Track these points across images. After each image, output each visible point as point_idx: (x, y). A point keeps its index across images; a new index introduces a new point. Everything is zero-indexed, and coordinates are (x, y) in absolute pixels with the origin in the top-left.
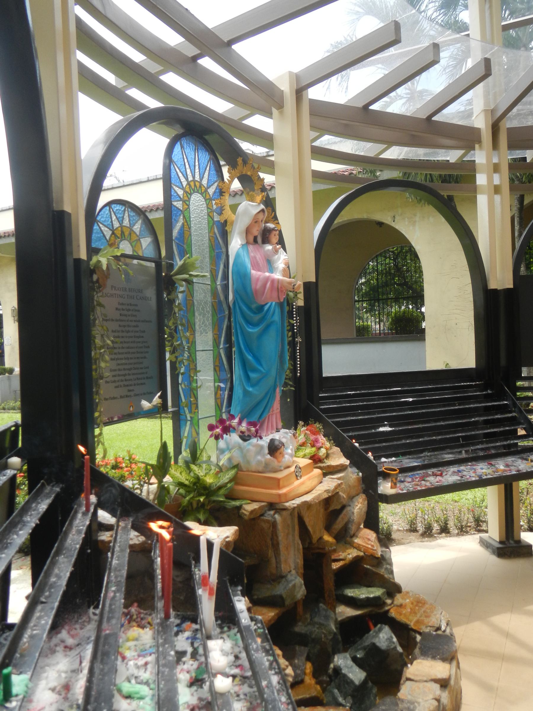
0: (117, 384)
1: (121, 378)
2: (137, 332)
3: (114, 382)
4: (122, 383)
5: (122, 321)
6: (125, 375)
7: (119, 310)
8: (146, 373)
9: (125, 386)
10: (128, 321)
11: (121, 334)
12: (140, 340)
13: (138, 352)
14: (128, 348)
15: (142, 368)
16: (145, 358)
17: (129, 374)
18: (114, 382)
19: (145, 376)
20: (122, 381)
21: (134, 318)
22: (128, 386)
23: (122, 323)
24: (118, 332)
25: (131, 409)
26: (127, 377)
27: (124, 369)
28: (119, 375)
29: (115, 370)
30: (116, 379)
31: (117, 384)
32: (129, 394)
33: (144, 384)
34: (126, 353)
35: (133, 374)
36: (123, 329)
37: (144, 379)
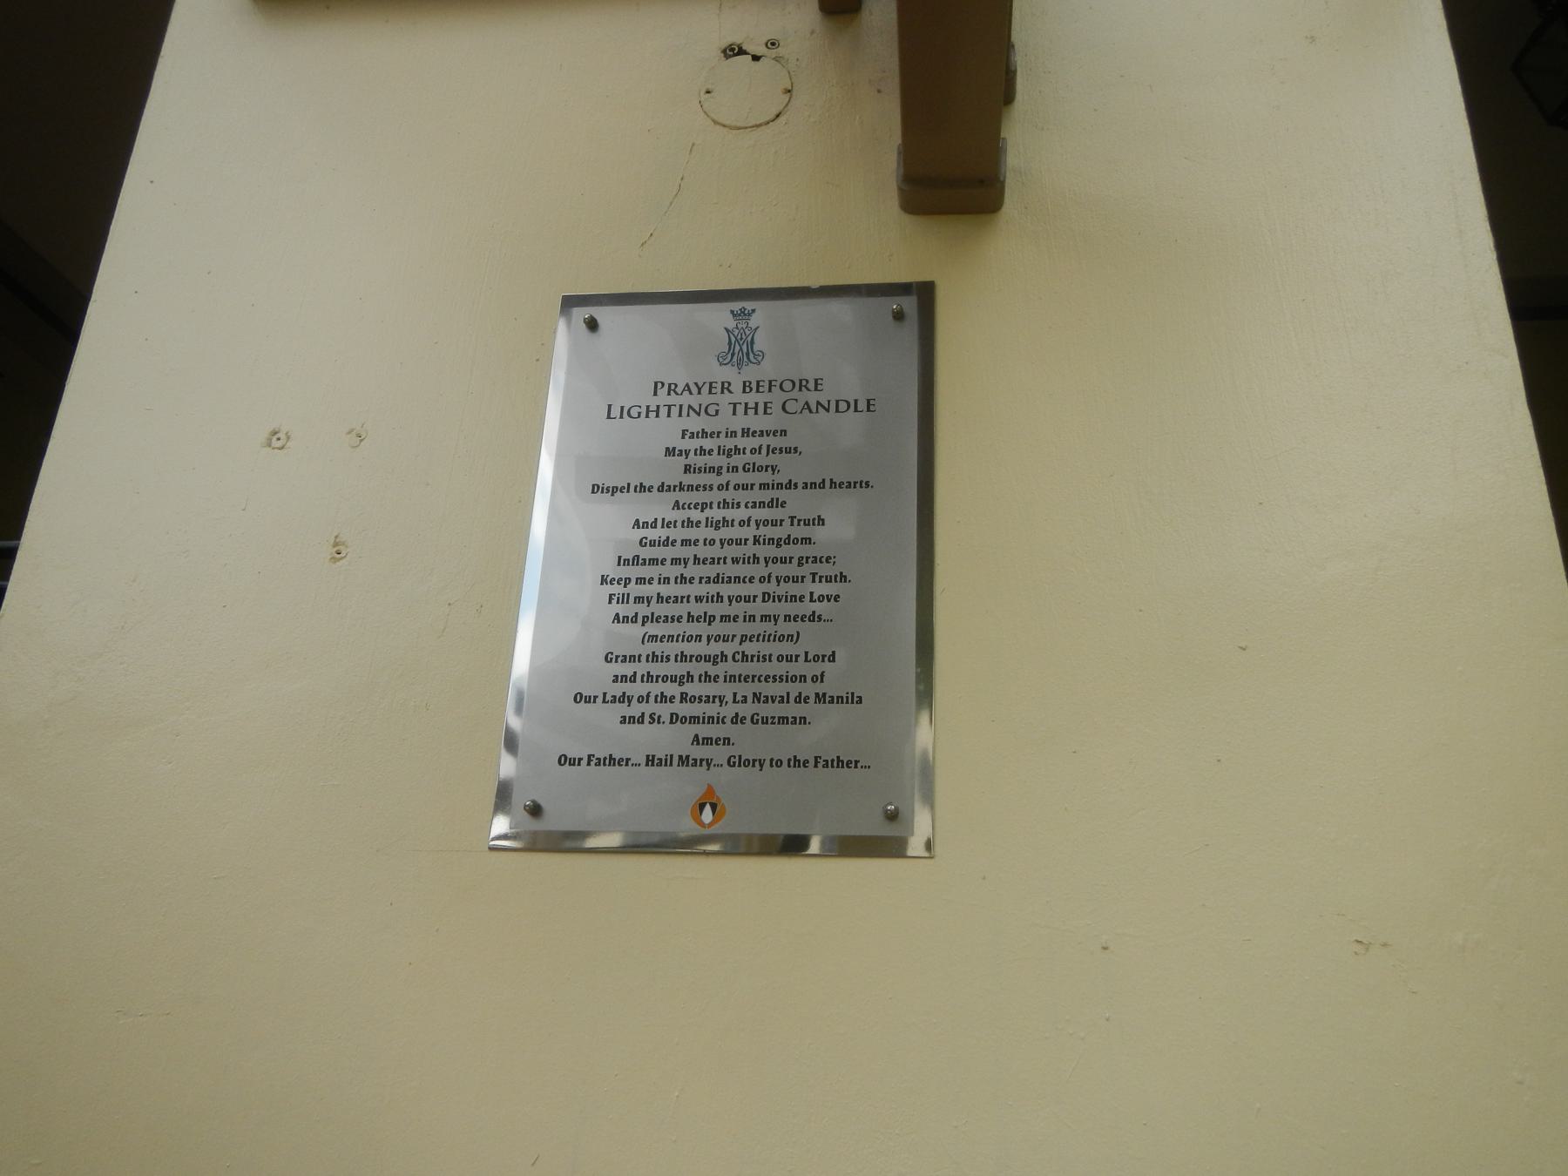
3: (624, 699)
4: (664, 710)
5: (690, 488)
6: (679, 680)
9: (674, 718)
11: (678, 534)
12: (796, 551)
13: (766, 597)
16: (813, 617)
18: (624, 699)
19: (809, 689)
20: (663, 698)
21: (766, 477)
23: (684, 497)
27: (683, 657)
29: (633, 659)
31: (636, 709)
33: (803, 720)
35: (732, 679)
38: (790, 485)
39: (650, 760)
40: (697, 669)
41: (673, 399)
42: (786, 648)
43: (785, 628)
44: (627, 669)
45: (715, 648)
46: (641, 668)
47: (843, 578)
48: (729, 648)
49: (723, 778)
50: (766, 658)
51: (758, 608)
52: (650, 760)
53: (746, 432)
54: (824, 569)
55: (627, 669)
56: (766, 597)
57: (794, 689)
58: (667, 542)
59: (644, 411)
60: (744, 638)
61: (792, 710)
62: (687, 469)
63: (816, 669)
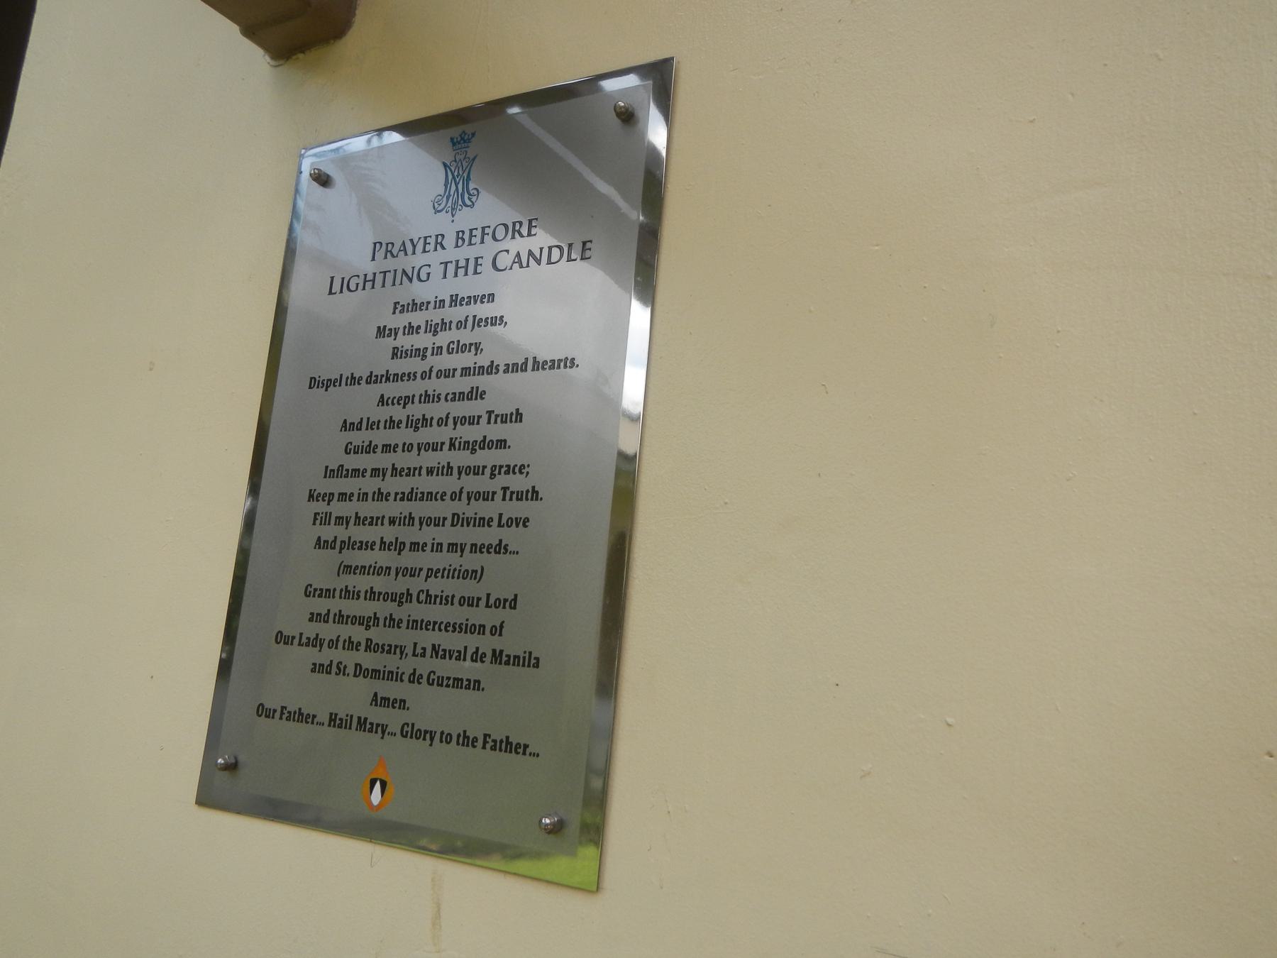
0: (326, 655)
1: (346, 631)
2: (473, 421)
3: (316, 642)
4: (350, 659)
6: (368, 622)
7: (394, 332)
8: (498, 630)
9: (359, 671)
13: (457, 520)
14: (410, 496)
15: (471, 602)
16: (501, 548)
17: (392, 622)
18: (316, 642)
19: (487, 643)
20: (351, 645)
22: (375, 674)
23: (392, 390)
24: (372, 425)
25: (376, 796)
26: (379, 635)
27: (372, 595)
28: (341, 618)
29: (327, 593)
30: (328, 631)
31: (326, 655)
32: (377, 715)
34: (392, 522)
36: (398, 413)
37: (478, 657)
39: (333, 719)
41: (390, 264)
45: (400, 585)
46: (335, 605)
47: (535, 494)
48: (416, 584)
50: (448, 600)
51: (446, 535)
52: (334, 720)
56: (457, 520)
59: (361, 281)
60: (432, 573)
61: (467, 669)
62: (395, 353)
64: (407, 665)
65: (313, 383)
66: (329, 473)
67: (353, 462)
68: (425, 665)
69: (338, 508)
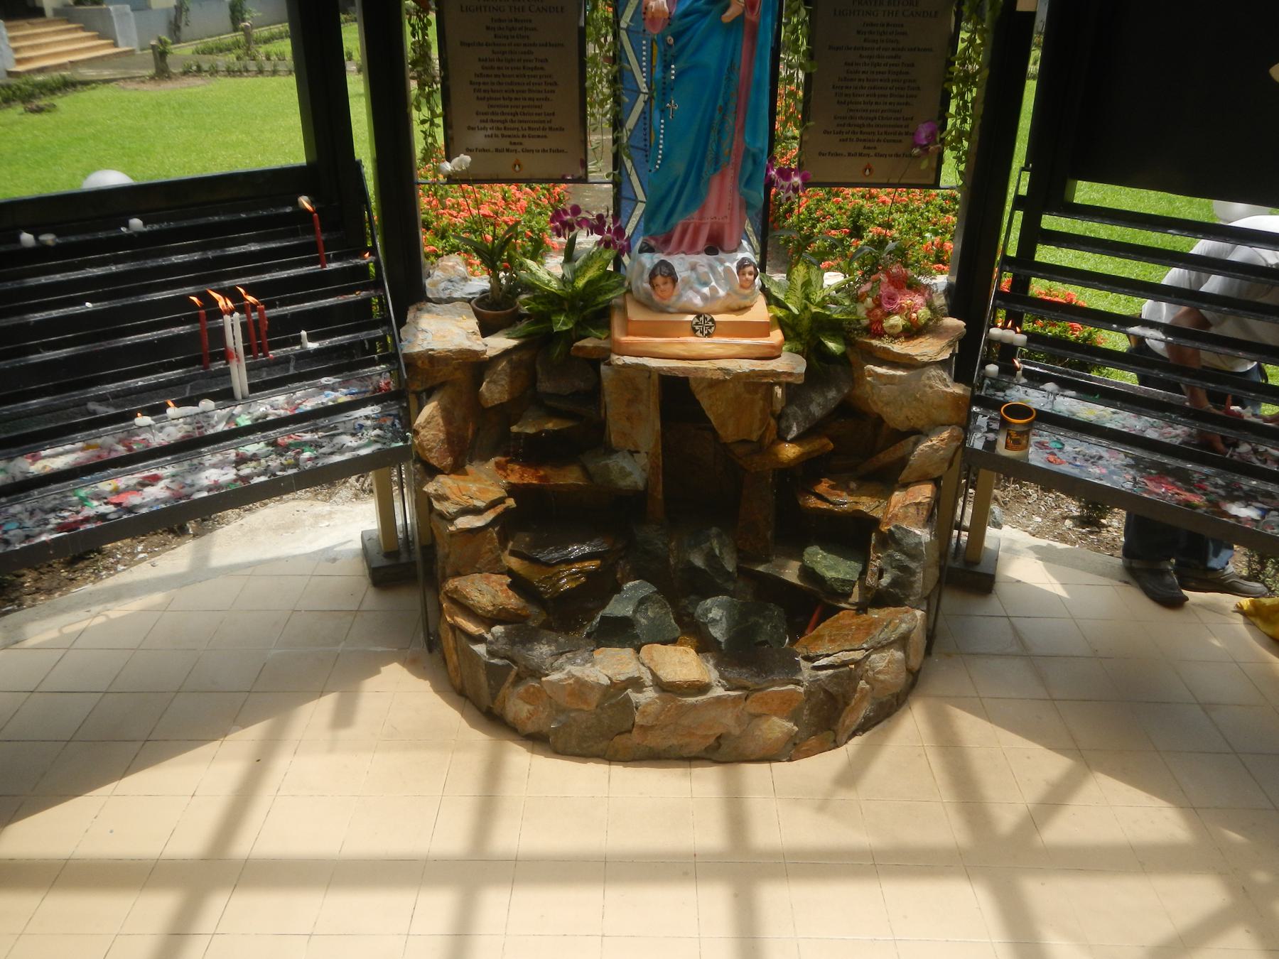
8: (550, 122)
10: (510, 45)
12: (539, 73)
14: (511, 84)
16: (547, 99)
18: (484, 128)
19: (547, 126)
31: (489, 132)
37: (544, 129)
38: (534, 45)
39: (497, 150)
40: (509, 118)
42: (538, 111)
43: (537, 103)
44: (484, 117)
45: (513, 110)
46: (489, 117)
48: (519, 110)
49: (522, 157)
51: (527, 95)
52: (497, 150)
53: (516, 20)
54: (549, 80)
55: (484, 117)
56: (530, 91)
57: (542, 125)
58: (492, 68)
61: (540, 133)
63: (548, 118)
64: (520, 133)
65: (462, 44)
66: (477, 75)
67: (485, 72)
68: (526, 133)
69: (483, 87)
